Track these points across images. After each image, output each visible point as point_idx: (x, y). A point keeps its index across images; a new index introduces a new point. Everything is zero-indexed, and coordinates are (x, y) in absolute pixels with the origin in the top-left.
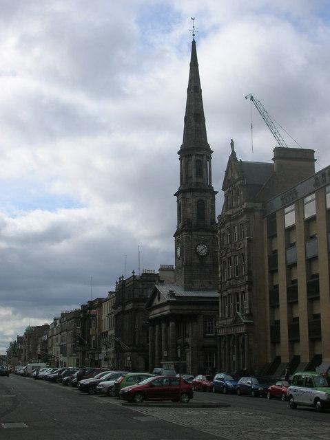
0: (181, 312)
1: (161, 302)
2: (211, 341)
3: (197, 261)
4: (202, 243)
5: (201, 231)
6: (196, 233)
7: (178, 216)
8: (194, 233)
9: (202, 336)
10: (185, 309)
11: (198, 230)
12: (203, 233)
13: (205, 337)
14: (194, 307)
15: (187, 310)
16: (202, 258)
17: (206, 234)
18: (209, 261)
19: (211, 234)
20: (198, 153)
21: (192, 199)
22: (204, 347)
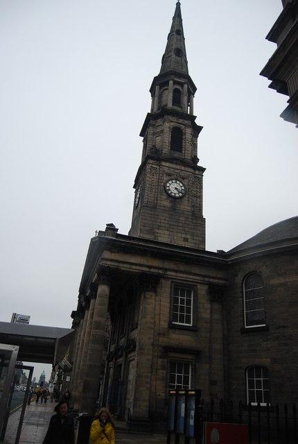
0: (124, 267)
2: (185, 339)
3: (167, 204)
4: (176, 180)
5: (176, 164)
6: (167, 164)
7: (143, 153)
8: (164, 163)
9: (165, 325)
10: (136, 263)
11: (166, 160)
12: (178, 167)
13: (171, 327)
14: (156, 263)
15: (136, 265)
16: (174, 199)
17: (183, 168)
18: (185, 206)
19: (190, 170)
20: (176, 79)
21: (167, 126)
22: (167, 350)
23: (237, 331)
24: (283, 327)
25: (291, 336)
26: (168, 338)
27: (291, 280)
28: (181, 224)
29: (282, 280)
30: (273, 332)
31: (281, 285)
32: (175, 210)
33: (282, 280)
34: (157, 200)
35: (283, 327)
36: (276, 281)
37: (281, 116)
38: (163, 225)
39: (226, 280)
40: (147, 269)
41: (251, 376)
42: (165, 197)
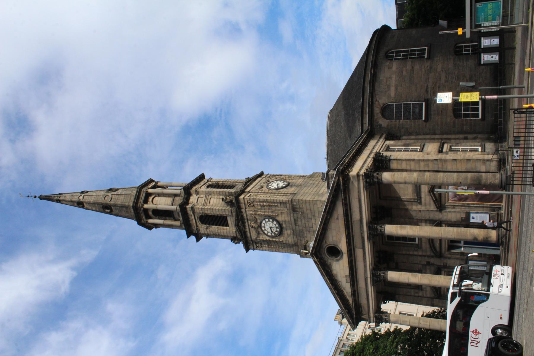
1: (343, 246)
8: (247, 190)
18: (300, 181)
23: (426, 125)
24: (427, 89)
25: (433, 83)
26: (431, 152)
27: (394, 82)
28: (317, 183)
29: (393, 89)
30: (429, 96)
31: (396, 88)
32: (300, 185)
33: (393, 89)
34: (287, 194)
35: (427, 89)
36: (392, 93)
37: (203, 173)
38: (315, 190)
39: (382, 134)
40: (369, 159)
41: (459, 116)
42: (285, 190)
